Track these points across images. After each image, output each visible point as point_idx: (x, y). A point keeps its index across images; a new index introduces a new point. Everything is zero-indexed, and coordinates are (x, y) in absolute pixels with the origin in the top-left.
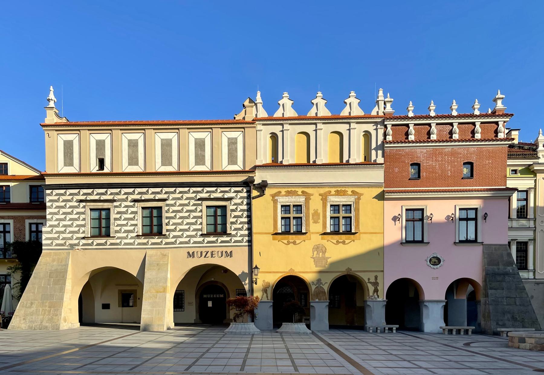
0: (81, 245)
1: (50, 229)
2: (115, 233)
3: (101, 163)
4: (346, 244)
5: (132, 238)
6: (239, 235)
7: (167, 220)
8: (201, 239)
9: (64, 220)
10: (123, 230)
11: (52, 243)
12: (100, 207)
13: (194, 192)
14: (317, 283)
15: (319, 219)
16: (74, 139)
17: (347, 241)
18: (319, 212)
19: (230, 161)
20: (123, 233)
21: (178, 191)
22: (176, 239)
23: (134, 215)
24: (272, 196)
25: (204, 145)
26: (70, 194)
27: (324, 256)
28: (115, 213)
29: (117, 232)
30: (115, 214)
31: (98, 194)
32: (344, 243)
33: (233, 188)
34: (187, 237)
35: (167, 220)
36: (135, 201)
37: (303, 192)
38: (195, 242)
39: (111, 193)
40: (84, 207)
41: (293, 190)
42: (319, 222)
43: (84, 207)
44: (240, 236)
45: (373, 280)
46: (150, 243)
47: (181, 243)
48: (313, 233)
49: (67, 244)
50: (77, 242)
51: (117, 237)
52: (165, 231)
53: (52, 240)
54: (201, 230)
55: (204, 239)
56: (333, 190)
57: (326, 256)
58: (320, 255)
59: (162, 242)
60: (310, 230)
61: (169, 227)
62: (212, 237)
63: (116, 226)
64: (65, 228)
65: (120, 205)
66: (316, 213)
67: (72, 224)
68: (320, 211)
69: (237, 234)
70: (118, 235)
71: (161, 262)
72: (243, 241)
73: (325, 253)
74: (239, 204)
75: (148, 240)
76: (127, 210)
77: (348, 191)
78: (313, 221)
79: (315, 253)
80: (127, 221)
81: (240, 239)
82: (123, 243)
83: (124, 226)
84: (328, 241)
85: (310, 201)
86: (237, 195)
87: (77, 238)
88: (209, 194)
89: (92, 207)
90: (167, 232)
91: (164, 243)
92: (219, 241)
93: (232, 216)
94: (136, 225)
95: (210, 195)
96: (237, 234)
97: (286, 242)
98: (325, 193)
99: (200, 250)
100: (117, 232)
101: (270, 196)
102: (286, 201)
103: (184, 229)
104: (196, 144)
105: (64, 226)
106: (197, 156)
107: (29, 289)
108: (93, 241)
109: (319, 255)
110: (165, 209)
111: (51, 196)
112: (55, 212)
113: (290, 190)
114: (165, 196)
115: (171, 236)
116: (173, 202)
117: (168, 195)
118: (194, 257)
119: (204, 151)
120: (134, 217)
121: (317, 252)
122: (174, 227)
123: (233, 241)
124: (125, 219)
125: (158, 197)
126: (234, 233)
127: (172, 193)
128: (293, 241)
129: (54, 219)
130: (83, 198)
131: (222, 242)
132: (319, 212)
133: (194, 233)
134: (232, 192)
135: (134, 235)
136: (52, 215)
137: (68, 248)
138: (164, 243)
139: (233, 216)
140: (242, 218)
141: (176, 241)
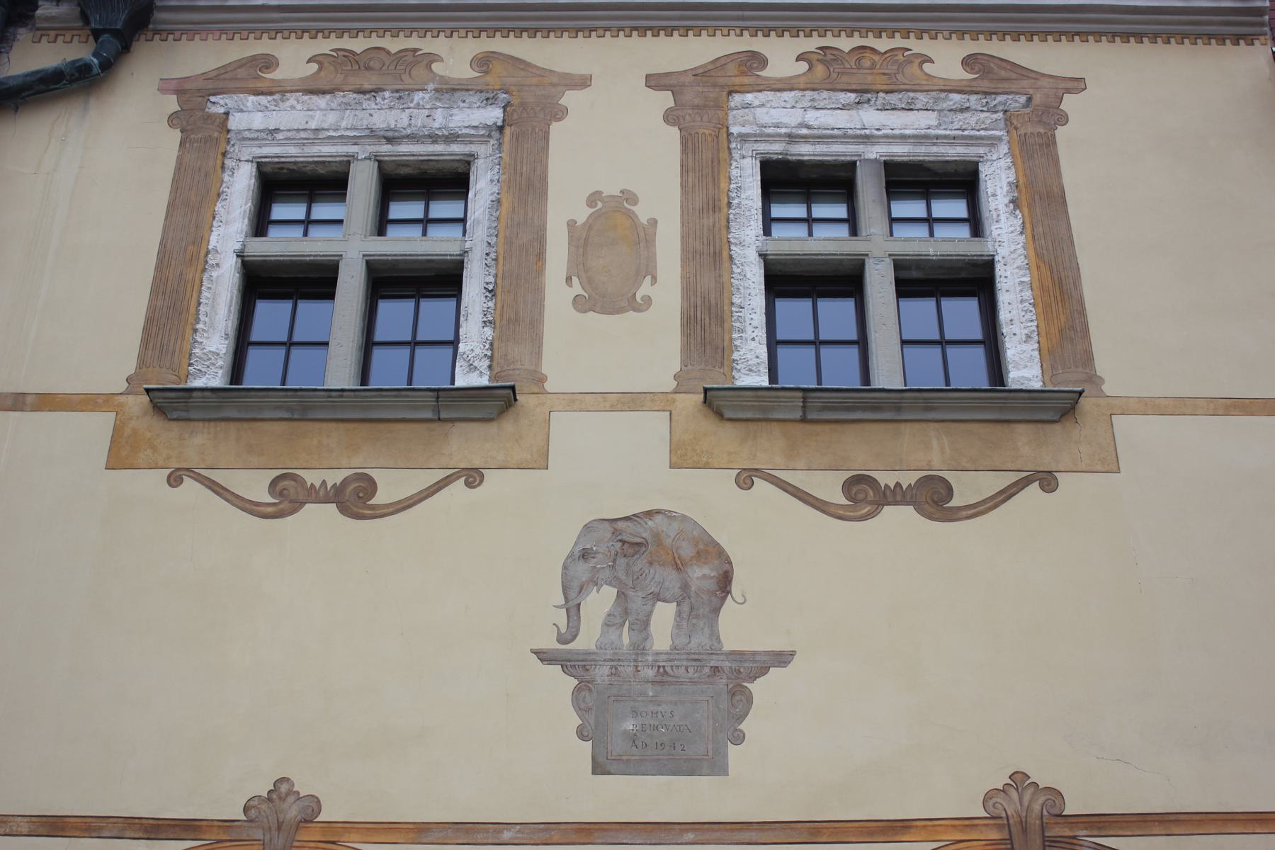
4: (953, 515)
15: (648, 269)
18: (643, 219)
24: (180, 92)
27: (699, 641)
37: (484, 62)
41: (394, 45)
42: (648, 301)
48: (575, 401)
57: (728, 646)
58: (653, 627)
60: (546, 369)
73: (717, 610)
77: (931, 61)
78: (577, 289)
79: (599, 603)
84: (745, 480)
85: (555, 128)
97: (256, 486)
98: (703, 74)
101: (163, 90)
102: (313, 125)
109: (643, 625)
113: (358, 45)
121: (621, 595)
128: (335, 477)
132: (643, 213)
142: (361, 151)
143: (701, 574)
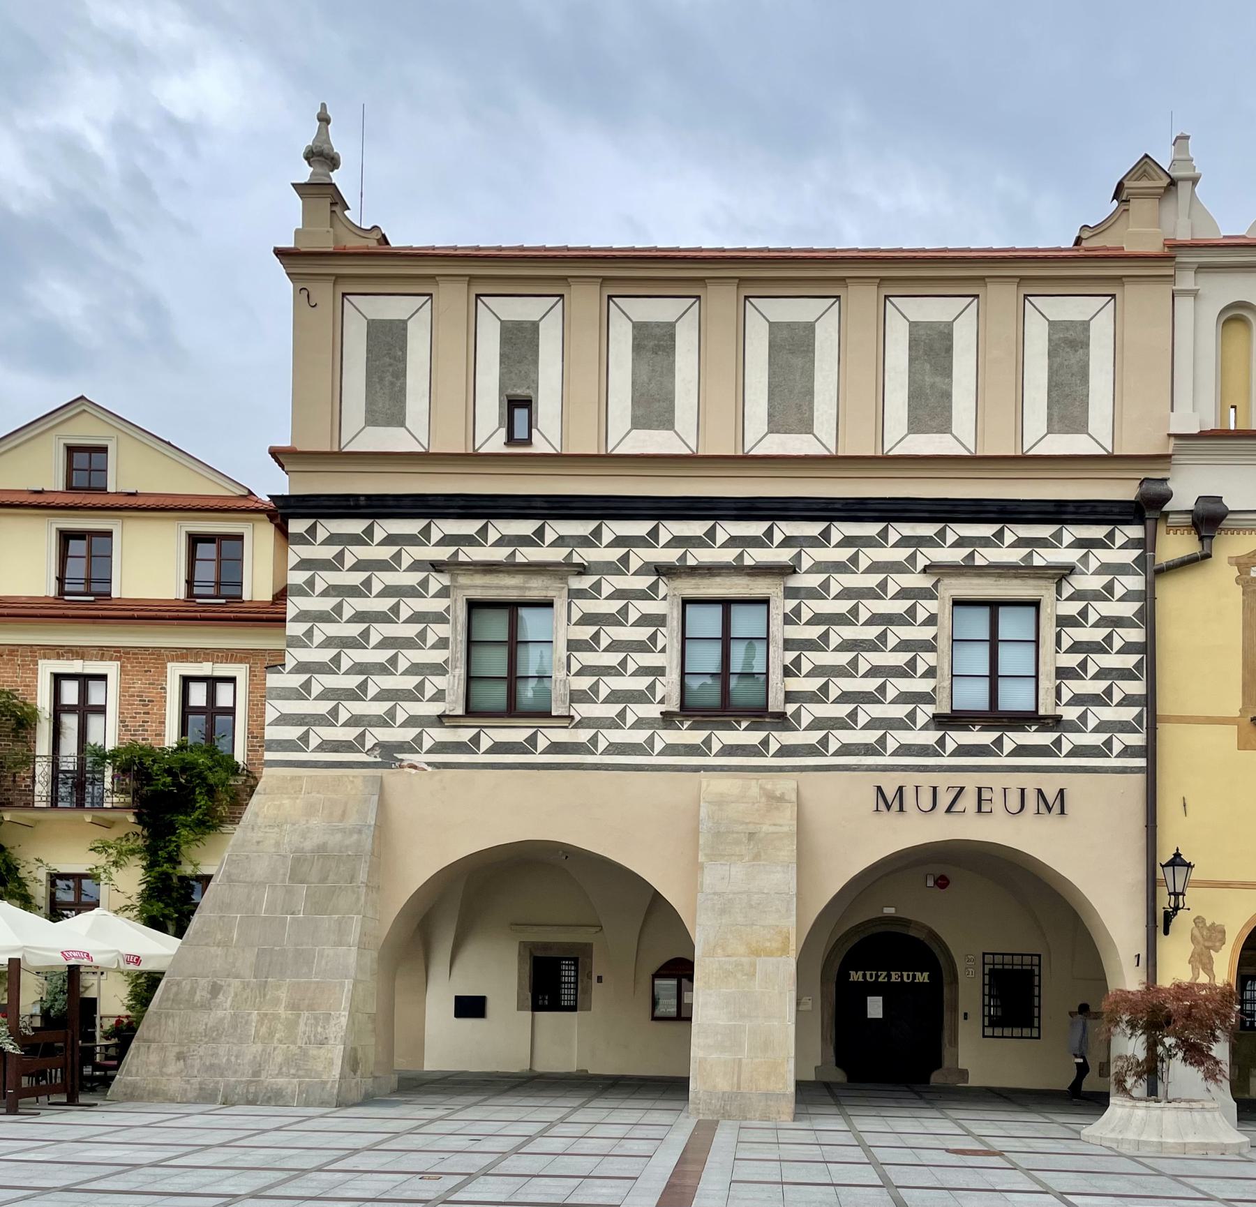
0: (425, 749)
1: (297, 680)
2: (572, 701)
5: (640, 724)
6: (1092, 722)
7: (791, 656)
8: (931, 737)
9: (359, 642)
10: (604, 692)
11: (305, 738)
12: (513, 595)
13: (904, 542)
16: (410, 318)
19: (1056, 418)
20: (605, 701)
21: (836, 537)
22: (825, 732)
23: (653, 629)
24: (1238, 565)
25: (949, 349)
26: (390, 540)
28: (573, 621)
29: (577, 697)
30: (575, 624)
31: (502, 541)
33: (1070, 527)
34: (873, 724)
35: (791, 656)
38: (904, 750)
39: (561, 538)
40: (444, 592)
43: (444, 592)
44: (1096, 730)
46: (716, 746)
47: (845, 750)
49: (368, 745)
50: (409, 734)
51: (577, 718)
52: (781, 696)
53: (306, 724)
54: (927, 698)
55: (944, 736)
59: (765, 743)
61: (795, 684)
62: (978, 728)
63: (577, 674)
64: (362, 678)
65: (597, 587)
67: (393, 660)
69: (1083, 718)
70: (582, 710)
71: (765, 828)
72: (1111, 750)
74: (1097, 596)
75: (706, 733)
76: (624, 611)
80: (625, 654)
81: (1098, 739)
82: (602, 745)
83: (609, 675)
86: (1086, 555)
87: (412, 721)
88: (968, 550)
89: (477, 594)
90: (788, 705)
91: (774, 746)
92: (1008, 746)
93: (1065, 645)
94: (659, 671)
95: (971, 556)
96: (1083, 718)
99: (926, 780)
100: (577, 697)
103: (860, 692)
104: (913, 343)
105: (358, 668)
106: (916, 396)
107: (205, 930)
108: (478, 734)
110: (779, 606)
111: (310, 543)
112: (322, 612)
114: (784, 556)
115: (806, 719)
116: (814, 581)
117: (795, 551)
119: (947, 372)
120: (653, 638)
122: (820, 681)
123: (1066, 747)
124: (614, 646)
125: (755, 556)
126: (1071, 713)
127: (813, 542)
129: (318, 638)
130: (444, 554)
131: (1020, 751)
133: (901, 711)
134: (1065, 543)
136: (311, 624)
137: (372, 759)
138: (774, 746)
139: (1066, 643)
140: (1106, 652)
141: (824, 742)
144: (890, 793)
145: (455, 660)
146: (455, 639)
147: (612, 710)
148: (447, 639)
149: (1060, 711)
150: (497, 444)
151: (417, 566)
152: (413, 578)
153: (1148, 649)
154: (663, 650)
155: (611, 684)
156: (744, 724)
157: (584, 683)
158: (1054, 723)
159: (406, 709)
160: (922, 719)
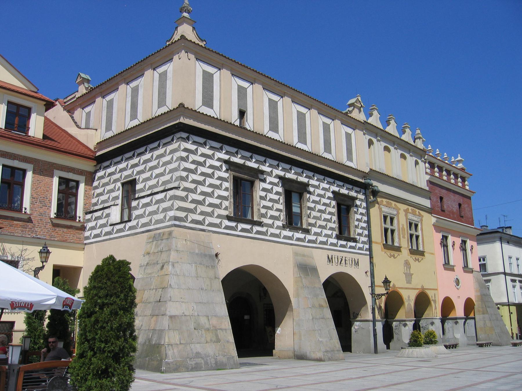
3: (242, 114)
5: (278, 227)
7: (309, 211)
8: (335, 241)
11: (186, 217)
14: (408, 300)
15: (405, 234)
17: (420, 259)
29: (264, 216)
32: (418, 260)
36: (280, 178)
38: (332, 244)
43: (227, 171)
45: (433, 298)
56: (410, 208)
63: (262, 208)
66: (403, 229)
68: (405, 227)
85: (399, 215)
87: (219, 216)
97: (389, 254)
98: (406, 210)
100: (264, 216)
118: (332, 262)
126: (358, 237)
133: (329, 232)
135: (280, 223)
142: (389, 215)
143: (409, 266)
144: (330, 257)
145: (231, 196)
146: (230, 188)
147: (270, 222)
148: (228, 188)
149: (357, 237)
150: (237, 123)
151: (219, 160)
152: (218, 164)
153: (368, 222)
154: (281, 204)
155: (271, 213)
156: (300, 232)
157: (263, 211)
158: (355, 240)
159: (217, 212)
160: (334, 236)
